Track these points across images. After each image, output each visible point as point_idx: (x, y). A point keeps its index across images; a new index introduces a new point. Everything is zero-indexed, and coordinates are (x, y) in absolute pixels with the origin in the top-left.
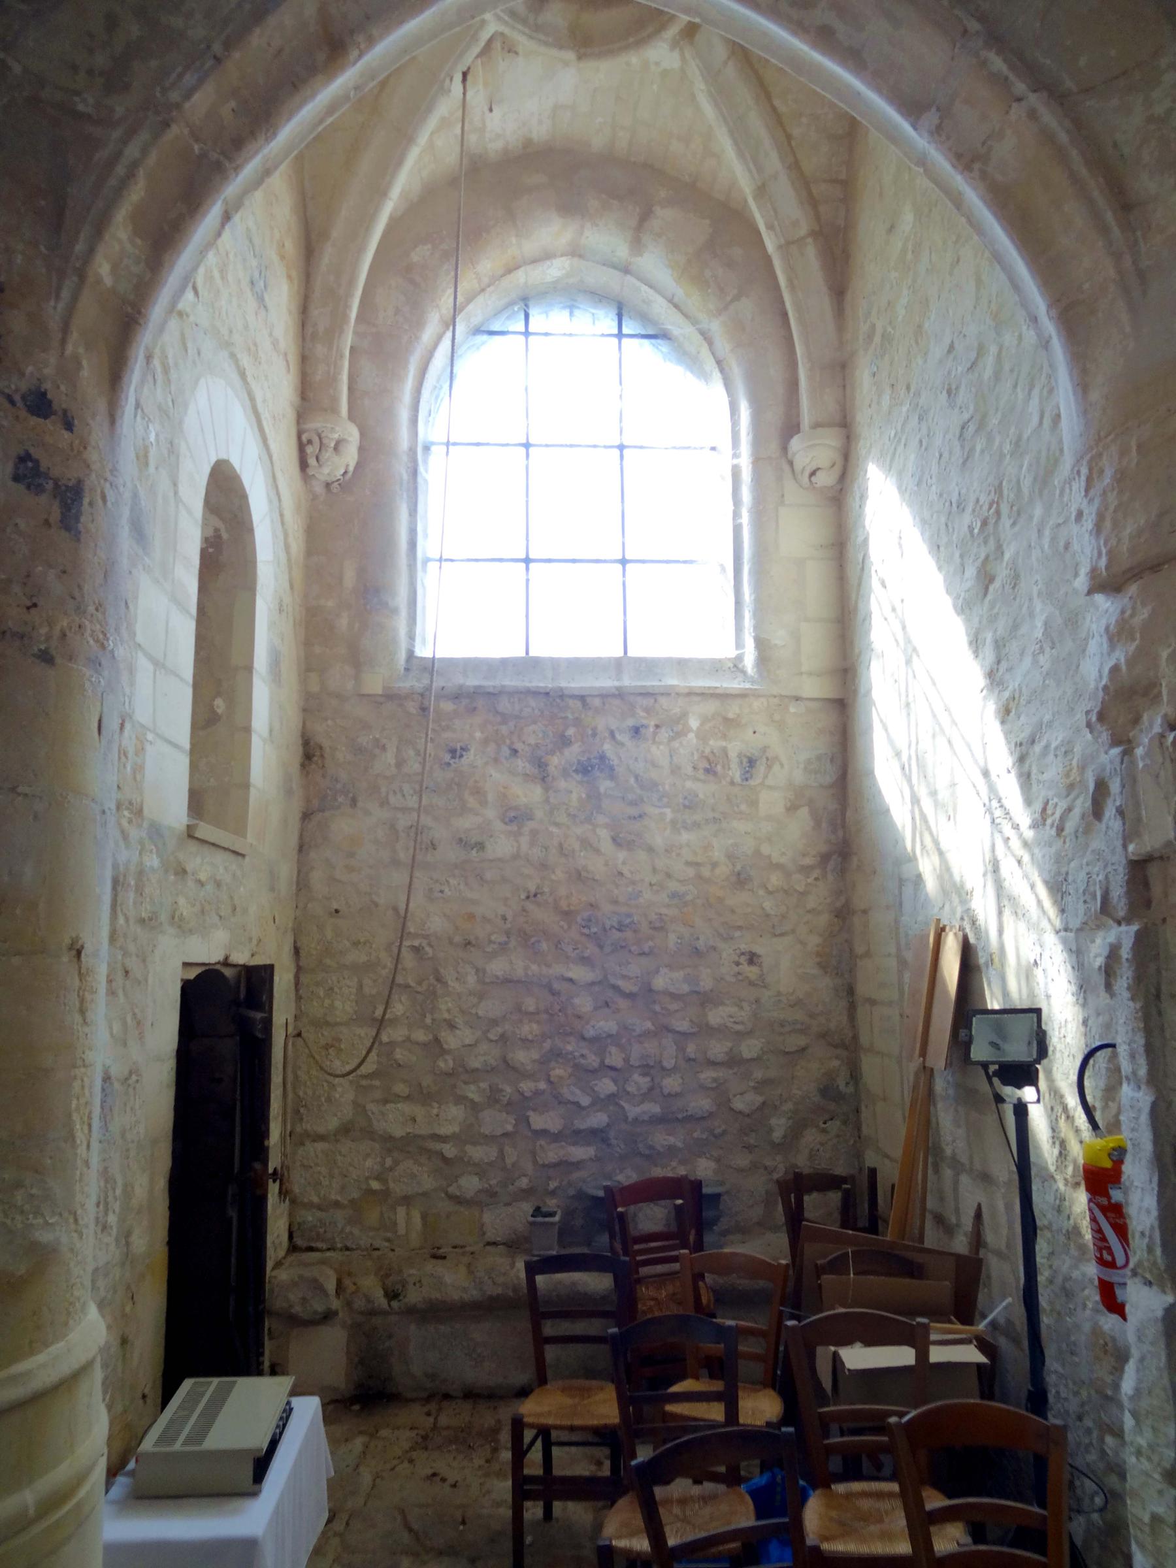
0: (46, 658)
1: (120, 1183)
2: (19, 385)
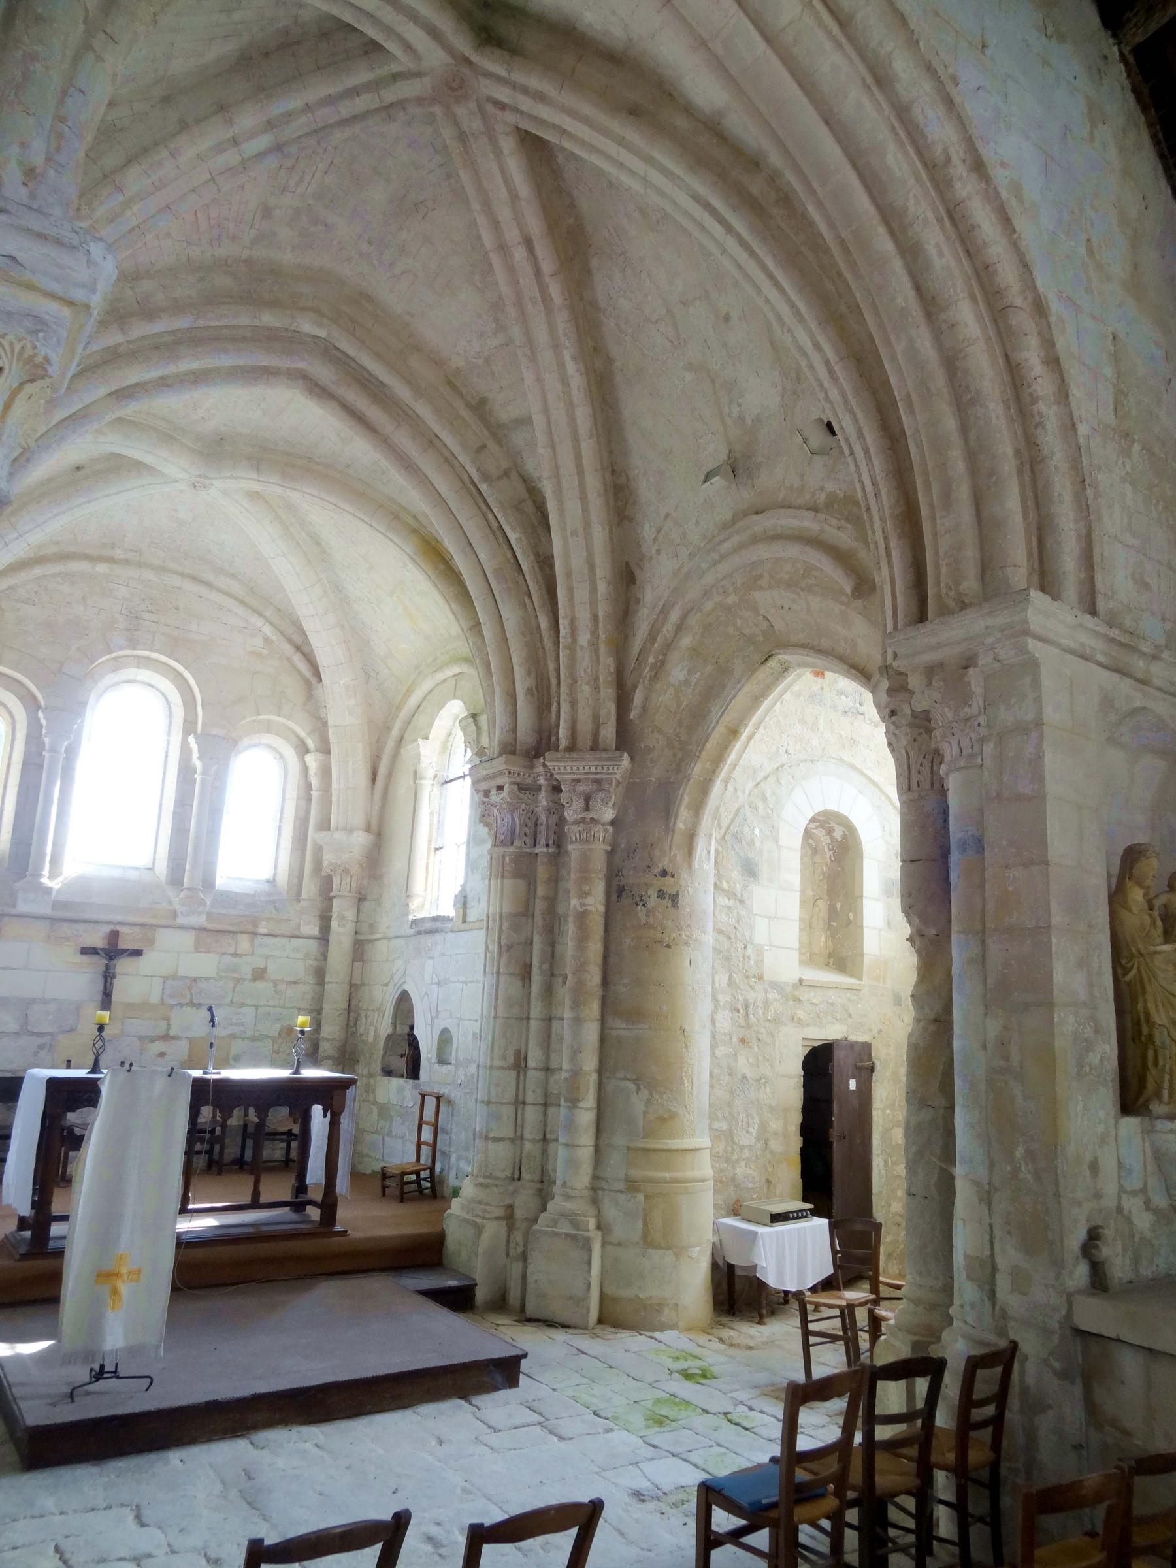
0: (668, 946)
1: (757, 1120)
2: (657, 870)
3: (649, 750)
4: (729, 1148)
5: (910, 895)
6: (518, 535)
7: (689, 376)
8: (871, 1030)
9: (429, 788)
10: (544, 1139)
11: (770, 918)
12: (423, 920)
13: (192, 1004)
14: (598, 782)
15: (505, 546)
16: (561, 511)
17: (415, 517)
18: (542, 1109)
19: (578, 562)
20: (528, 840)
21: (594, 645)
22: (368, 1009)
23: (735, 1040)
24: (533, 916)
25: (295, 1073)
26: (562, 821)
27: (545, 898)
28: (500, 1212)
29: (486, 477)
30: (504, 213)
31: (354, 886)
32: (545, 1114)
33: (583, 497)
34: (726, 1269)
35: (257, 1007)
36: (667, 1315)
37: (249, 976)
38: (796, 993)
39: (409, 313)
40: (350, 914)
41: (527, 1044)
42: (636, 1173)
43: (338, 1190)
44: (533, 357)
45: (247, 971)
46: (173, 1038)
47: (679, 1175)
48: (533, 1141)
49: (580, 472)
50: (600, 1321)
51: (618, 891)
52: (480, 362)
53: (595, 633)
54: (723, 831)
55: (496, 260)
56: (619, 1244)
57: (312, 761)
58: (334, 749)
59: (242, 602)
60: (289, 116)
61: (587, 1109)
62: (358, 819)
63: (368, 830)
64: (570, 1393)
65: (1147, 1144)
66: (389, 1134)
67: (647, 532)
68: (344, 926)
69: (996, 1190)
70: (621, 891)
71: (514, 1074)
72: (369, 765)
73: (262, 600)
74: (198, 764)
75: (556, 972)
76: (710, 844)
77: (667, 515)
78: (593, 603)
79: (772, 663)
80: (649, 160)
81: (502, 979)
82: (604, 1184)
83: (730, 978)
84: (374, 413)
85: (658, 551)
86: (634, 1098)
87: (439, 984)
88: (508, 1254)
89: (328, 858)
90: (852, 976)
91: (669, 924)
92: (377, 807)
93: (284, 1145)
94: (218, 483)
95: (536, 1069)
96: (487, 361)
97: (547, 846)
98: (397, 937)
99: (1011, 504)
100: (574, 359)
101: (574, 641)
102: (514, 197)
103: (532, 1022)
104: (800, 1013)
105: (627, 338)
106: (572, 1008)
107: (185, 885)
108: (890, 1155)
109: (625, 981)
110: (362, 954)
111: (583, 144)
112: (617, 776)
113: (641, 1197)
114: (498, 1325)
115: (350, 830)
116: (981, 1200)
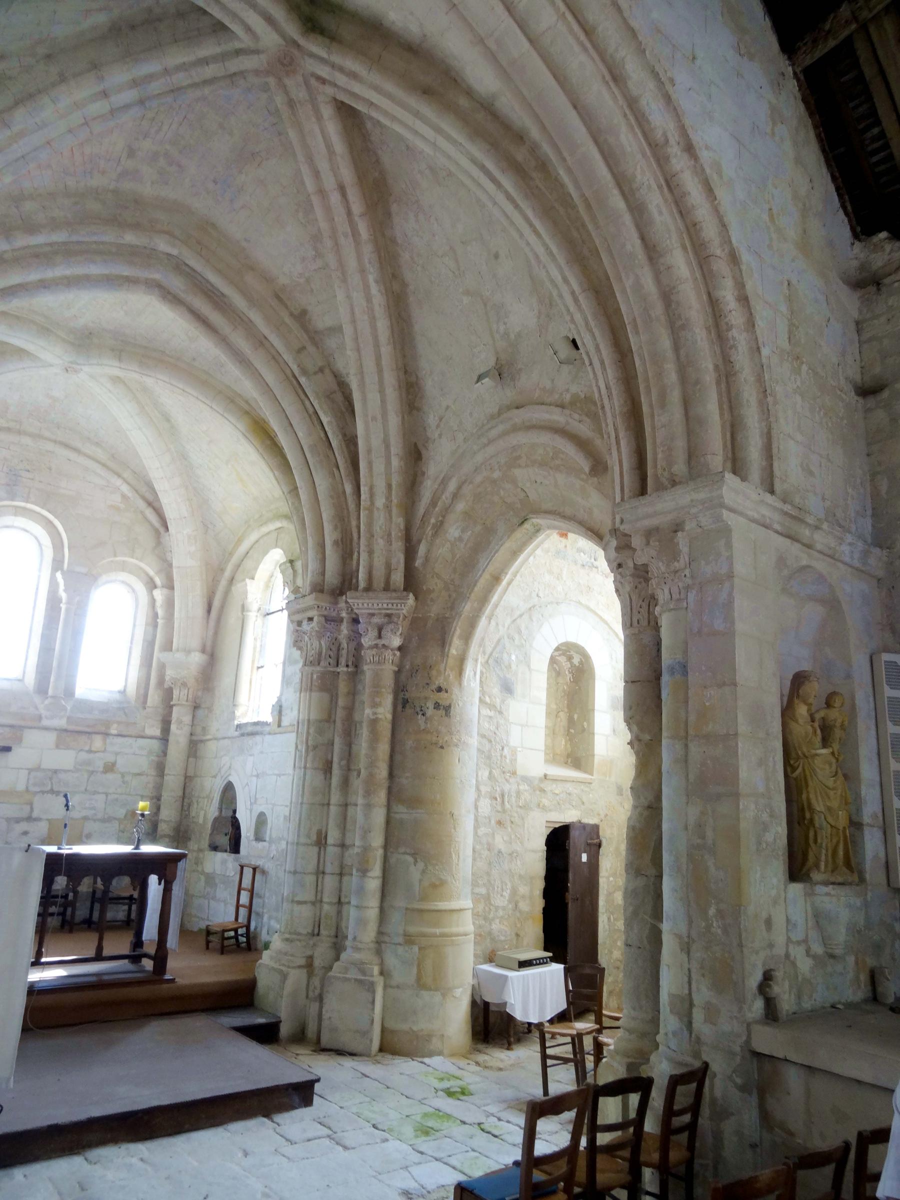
0: (442, 747)
1: (509, 886)
2: (434, 687)
3: (430, 591)
4: (487, 909)
5: (631, 708)
6: (329, 419)
7: (466, 300)
8: (599, 815)
9: (254, 619)
10: (340, 902)
11: (522, 726)
12: (247, 724)
13: (52, 791)
14: (389, 616)
15: (319, 427)
16: (364, 400)
17: (247, 402)
18: (337, 878)
19: (376, 442)
20: (331, 661)
21: (388, 507)
22: (199, 797)
23: (493, 822)
24: (335, 722)
25: (135, 849)
26: (359, 647)
27: (344, 708)
28: (302, 962)
29: (304, 372)
30: (323, 166)
31: (190, 696)
32: (340, 882)
33: (382, 391)
34: (482, 1006)
35: (107, 794)
36: (435, 1043)
37: (101, 769)
38: (542, 785)
39: (245, 240)
40: (187, 719)
41: (327, 825)
42: (412, 929)
43: (168, 945)
44: (344, 280)
45: (99, 765)
46: (38, 819)
47: (446, 930)
48: (330, 903)
49: (380, 371)
50: (381, 1050)
51: (403, 703)
52: (302, 280)
53: (388, 498)
54: (486, 657)
55: (315, 200)
56: (398, 987)
57: (159, 594)
58: (177, 585)
59: (104, 465)
60: (150, 78)
61: (373, 878)
62: (195, 643)
63: (203, 651)
64: (354, 1110)
65: (808, 904)
66: (214, 898)
67: (431, 420)
68: (181, 729)
69: (694, 941)
70: (405, 702)
71: (316, 849)
72: (205, 599)
73: (120, 464)
74: (63, 595)
75: (353, 768)
76: (476, 666)
77: (448, 407)
78: (388, 474)
79: (527, 526)
80: (438, 130)
81: (309, 772)
82: (386, 939)
83: (490, 773)
84: (216, 318)
85: (440, 436)
86: (412, 868)
87: (257, 776)
88: (307, 997)
89: (170, 673)
90: (585, 772)
91: (443, 730)
92: (211, 633)
93: (126, 907)
94: (86, 369)
95: (334, 845)
96: (308, 281)
97: (347, 666)
98: (225, 738)
99: (711, 408)
100: (376, 282)
101: (372, 503)
102: (331, 152)
103: (331, 807)
104: (545, 802)
105: (419, 268)
106: (364, 796)
107: (50, 692)
108: (612, 913)
109: (407, 775)
110: (196, 751)
111: (386, 113)
112: (404, 612)
113: (416, 949)
114: (297, 1054)
115: (188, 652)
116: (682, 950)
